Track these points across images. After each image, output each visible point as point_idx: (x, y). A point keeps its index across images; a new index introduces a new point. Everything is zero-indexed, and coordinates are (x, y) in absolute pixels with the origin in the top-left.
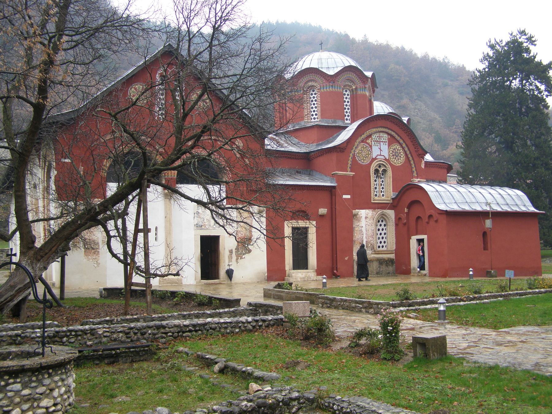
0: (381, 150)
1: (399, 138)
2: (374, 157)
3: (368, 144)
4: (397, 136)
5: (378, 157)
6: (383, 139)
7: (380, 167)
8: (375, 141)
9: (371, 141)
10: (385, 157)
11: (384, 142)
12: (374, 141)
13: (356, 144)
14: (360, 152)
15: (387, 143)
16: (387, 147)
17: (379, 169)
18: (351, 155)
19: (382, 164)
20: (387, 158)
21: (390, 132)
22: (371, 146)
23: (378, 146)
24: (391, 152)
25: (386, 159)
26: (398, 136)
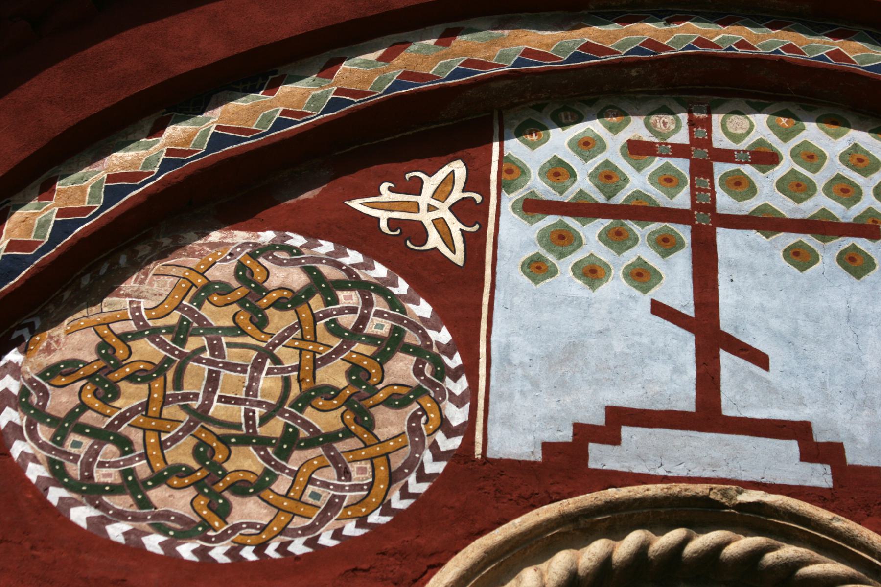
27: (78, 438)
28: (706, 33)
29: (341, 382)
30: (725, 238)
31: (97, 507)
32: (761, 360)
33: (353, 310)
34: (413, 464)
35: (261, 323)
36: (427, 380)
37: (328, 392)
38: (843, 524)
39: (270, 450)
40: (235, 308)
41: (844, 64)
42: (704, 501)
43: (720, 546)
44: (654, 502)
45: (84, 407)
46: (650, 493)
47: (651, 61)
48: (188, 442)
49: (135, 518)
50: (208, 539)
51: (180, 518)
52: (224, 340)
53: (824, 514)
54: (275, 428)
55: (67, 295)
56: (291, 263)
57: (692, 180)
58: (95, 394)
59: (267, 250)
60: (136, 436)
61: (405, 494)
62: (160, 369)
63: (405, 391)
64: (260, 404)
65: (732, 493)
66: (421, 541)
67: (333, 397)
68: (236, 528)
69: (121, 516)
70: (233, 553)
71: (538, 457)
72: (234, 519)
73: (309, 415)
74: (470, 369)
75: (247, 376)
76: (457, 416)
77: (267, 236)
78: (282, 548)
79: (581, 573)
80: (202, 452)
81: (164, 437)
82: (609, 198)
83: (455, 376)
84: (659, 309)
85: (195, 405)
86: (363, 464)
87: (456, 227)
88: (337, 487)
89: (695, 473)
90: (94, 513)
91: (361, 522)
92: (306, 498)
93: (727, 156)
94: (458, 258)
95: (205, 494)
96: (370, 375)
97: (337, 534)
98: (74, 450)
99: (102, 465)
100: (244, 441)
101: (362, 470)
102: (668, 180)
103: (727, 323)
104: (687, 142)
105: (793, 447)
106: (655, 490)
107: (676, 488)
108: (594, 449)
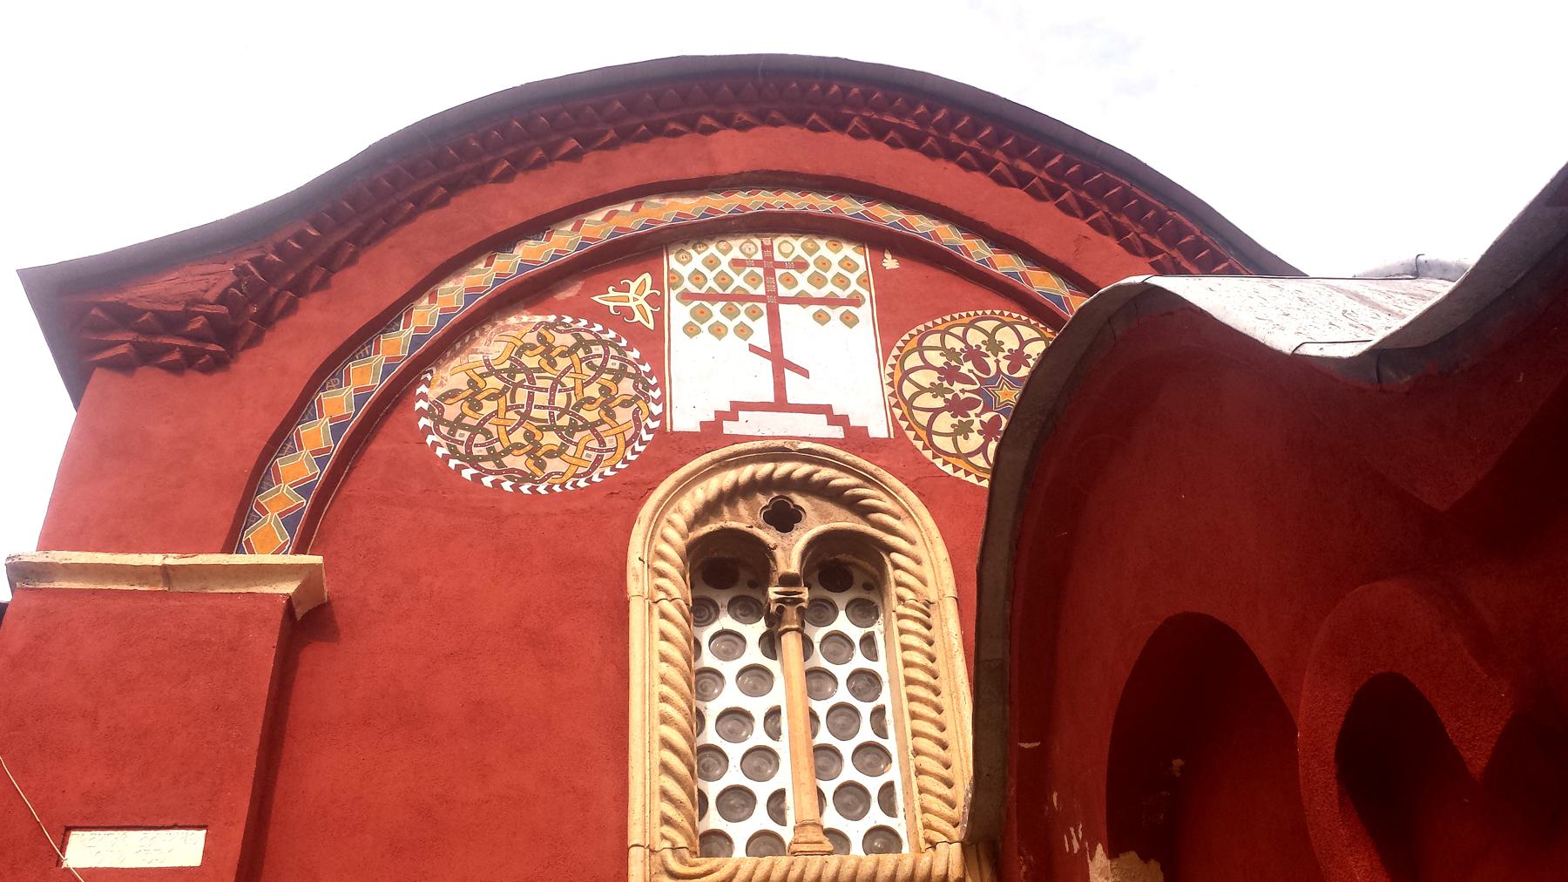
0: (780, 365)
1: (1006, 265)
2: (686, 420)
3: (620, 319)
4: (977, 251)
5: (747, 425)
6: (817, 280)
7: (784, 518)
8: (712, 297)
9: (656, 301)
10: (842, 421)
11: (832, 301)
12: (686, 297)
13: (426, 315)
14: (494, 383)
15: (865, 313)
16: (865, 333)
17: (769, 536)
18: (339, 402)
19: (806, 486)
20: (879, 429)
21: (887, 215)
22: (653, 342)
23: (744, 331)
24: (926, 378)
25: (857, 439)
26: (1002, 241)
27: (463, 432)
28: (768, 200)
29: (597, 395)
30: (783, 308)
31: (475, 469)
32: (805, 373)
33: (599, 356)
34: (636, 436)
35: (553, 364)
36: (640, 392)
37: (591, 400)
38: (850, 457)
39: (563, 433)
40: (539, 357)
41: (840, 215)
42: (783, 449)
43: (790, 473)
44: (758, 450)
45: (463, 415)
46: (755, 446)
47: (741, 216)
48: (521, 431)
49: (497, 473)
50: (535, 482)
51: (520, 472)
52: (535, 375)
53: (841, 453)
54: (565, 421)
55: (449, 353)
56: (566, 332)
57: (765, 279)
58: (469, 407)
59: (549, 326)
60: (493, 429)
61: (634, 452)
62: (502, 392)
63: (629, 398)
64: (556, 408)
65: (796, 444)
66: (643, 476)
67: (593, 403)
68: (550, 475)
69: (489, 472)
70: (549, 488)
71: (698, 429)
72: (547, 471)
73: (582, 413)
74: (661, 385)
75: (548, 394)
76: (657, 410)
77: (552, 318)
78: (574, 484)
79: (724, 489)
80: (529, 436)
81: (508, 429)
82: (724, 291)
83: (654, 388)
84: (754, 349)
85: (523, 411)
86: (611, 437)
87: (648, 309)
88: (599, 451)
89: (777, 434)
90: (476, 472)
91: (613, 468)
92: (584, 457)
93: (781, 265)
94: (651, 326)
95: (531, 458)
96: (611, 391)
97: (601, 475)
98: (460, 439)
99: (476, 446)
100: (549, 429)
101: (611, 441)
102: (752, 279)
103: (788, 354)
104: (761, 258)
105: (823, 418)
106: (758, 444)
107: (768, 443)
108: (725, 423)
